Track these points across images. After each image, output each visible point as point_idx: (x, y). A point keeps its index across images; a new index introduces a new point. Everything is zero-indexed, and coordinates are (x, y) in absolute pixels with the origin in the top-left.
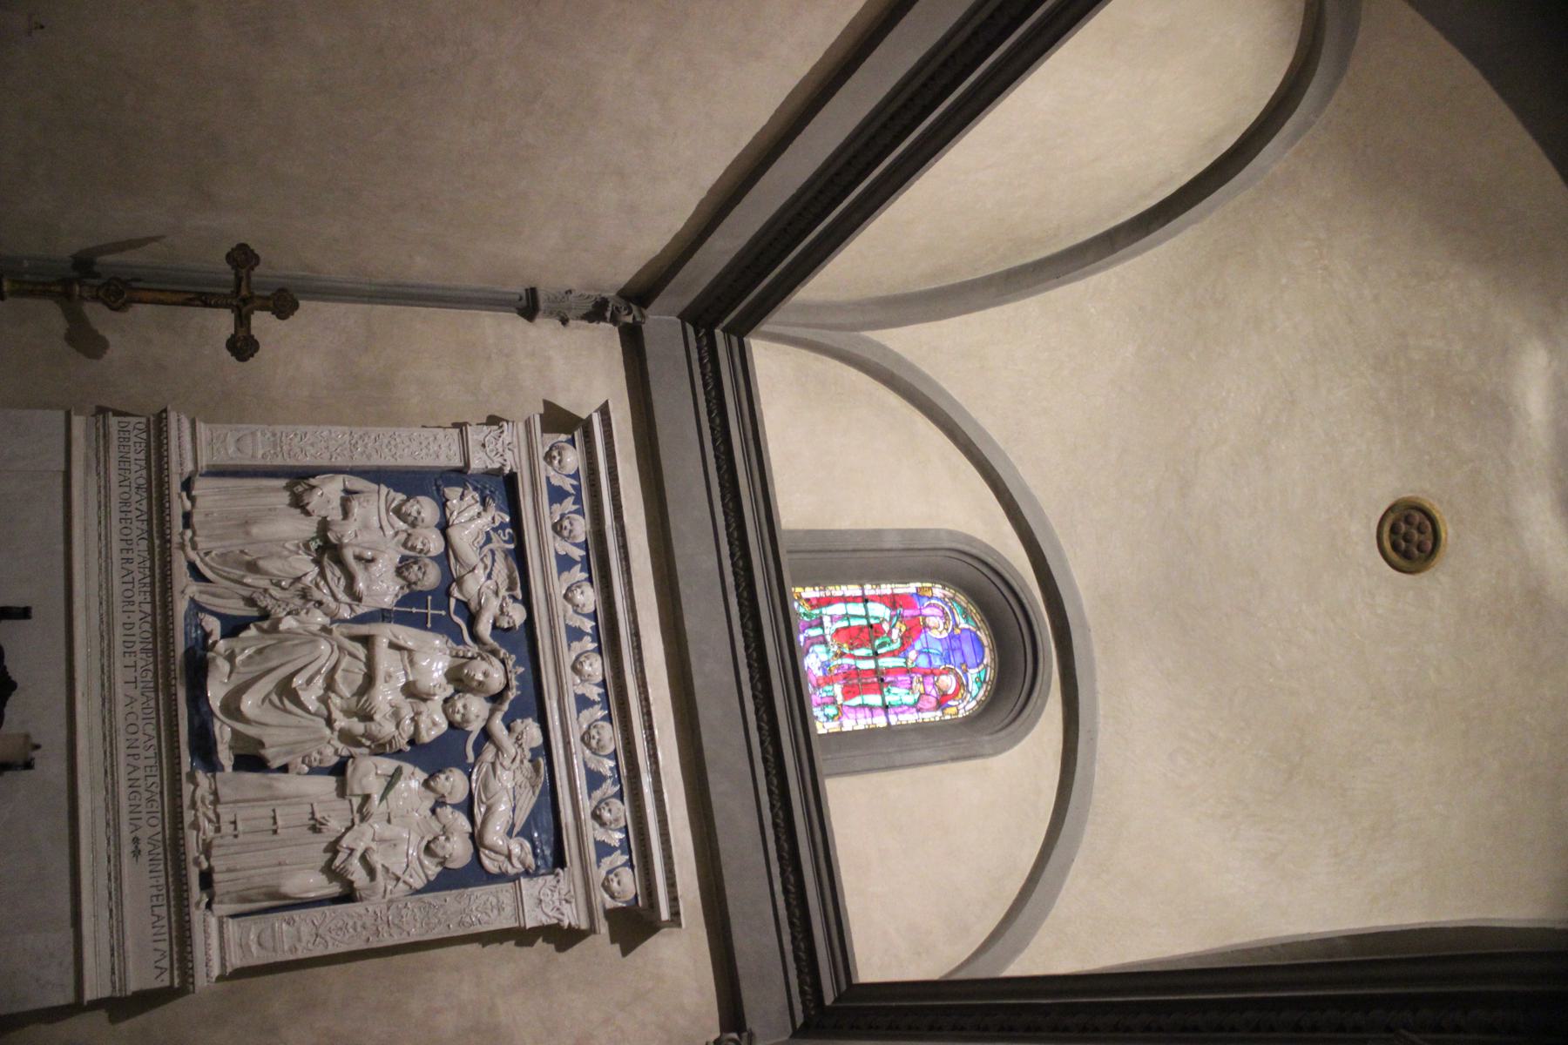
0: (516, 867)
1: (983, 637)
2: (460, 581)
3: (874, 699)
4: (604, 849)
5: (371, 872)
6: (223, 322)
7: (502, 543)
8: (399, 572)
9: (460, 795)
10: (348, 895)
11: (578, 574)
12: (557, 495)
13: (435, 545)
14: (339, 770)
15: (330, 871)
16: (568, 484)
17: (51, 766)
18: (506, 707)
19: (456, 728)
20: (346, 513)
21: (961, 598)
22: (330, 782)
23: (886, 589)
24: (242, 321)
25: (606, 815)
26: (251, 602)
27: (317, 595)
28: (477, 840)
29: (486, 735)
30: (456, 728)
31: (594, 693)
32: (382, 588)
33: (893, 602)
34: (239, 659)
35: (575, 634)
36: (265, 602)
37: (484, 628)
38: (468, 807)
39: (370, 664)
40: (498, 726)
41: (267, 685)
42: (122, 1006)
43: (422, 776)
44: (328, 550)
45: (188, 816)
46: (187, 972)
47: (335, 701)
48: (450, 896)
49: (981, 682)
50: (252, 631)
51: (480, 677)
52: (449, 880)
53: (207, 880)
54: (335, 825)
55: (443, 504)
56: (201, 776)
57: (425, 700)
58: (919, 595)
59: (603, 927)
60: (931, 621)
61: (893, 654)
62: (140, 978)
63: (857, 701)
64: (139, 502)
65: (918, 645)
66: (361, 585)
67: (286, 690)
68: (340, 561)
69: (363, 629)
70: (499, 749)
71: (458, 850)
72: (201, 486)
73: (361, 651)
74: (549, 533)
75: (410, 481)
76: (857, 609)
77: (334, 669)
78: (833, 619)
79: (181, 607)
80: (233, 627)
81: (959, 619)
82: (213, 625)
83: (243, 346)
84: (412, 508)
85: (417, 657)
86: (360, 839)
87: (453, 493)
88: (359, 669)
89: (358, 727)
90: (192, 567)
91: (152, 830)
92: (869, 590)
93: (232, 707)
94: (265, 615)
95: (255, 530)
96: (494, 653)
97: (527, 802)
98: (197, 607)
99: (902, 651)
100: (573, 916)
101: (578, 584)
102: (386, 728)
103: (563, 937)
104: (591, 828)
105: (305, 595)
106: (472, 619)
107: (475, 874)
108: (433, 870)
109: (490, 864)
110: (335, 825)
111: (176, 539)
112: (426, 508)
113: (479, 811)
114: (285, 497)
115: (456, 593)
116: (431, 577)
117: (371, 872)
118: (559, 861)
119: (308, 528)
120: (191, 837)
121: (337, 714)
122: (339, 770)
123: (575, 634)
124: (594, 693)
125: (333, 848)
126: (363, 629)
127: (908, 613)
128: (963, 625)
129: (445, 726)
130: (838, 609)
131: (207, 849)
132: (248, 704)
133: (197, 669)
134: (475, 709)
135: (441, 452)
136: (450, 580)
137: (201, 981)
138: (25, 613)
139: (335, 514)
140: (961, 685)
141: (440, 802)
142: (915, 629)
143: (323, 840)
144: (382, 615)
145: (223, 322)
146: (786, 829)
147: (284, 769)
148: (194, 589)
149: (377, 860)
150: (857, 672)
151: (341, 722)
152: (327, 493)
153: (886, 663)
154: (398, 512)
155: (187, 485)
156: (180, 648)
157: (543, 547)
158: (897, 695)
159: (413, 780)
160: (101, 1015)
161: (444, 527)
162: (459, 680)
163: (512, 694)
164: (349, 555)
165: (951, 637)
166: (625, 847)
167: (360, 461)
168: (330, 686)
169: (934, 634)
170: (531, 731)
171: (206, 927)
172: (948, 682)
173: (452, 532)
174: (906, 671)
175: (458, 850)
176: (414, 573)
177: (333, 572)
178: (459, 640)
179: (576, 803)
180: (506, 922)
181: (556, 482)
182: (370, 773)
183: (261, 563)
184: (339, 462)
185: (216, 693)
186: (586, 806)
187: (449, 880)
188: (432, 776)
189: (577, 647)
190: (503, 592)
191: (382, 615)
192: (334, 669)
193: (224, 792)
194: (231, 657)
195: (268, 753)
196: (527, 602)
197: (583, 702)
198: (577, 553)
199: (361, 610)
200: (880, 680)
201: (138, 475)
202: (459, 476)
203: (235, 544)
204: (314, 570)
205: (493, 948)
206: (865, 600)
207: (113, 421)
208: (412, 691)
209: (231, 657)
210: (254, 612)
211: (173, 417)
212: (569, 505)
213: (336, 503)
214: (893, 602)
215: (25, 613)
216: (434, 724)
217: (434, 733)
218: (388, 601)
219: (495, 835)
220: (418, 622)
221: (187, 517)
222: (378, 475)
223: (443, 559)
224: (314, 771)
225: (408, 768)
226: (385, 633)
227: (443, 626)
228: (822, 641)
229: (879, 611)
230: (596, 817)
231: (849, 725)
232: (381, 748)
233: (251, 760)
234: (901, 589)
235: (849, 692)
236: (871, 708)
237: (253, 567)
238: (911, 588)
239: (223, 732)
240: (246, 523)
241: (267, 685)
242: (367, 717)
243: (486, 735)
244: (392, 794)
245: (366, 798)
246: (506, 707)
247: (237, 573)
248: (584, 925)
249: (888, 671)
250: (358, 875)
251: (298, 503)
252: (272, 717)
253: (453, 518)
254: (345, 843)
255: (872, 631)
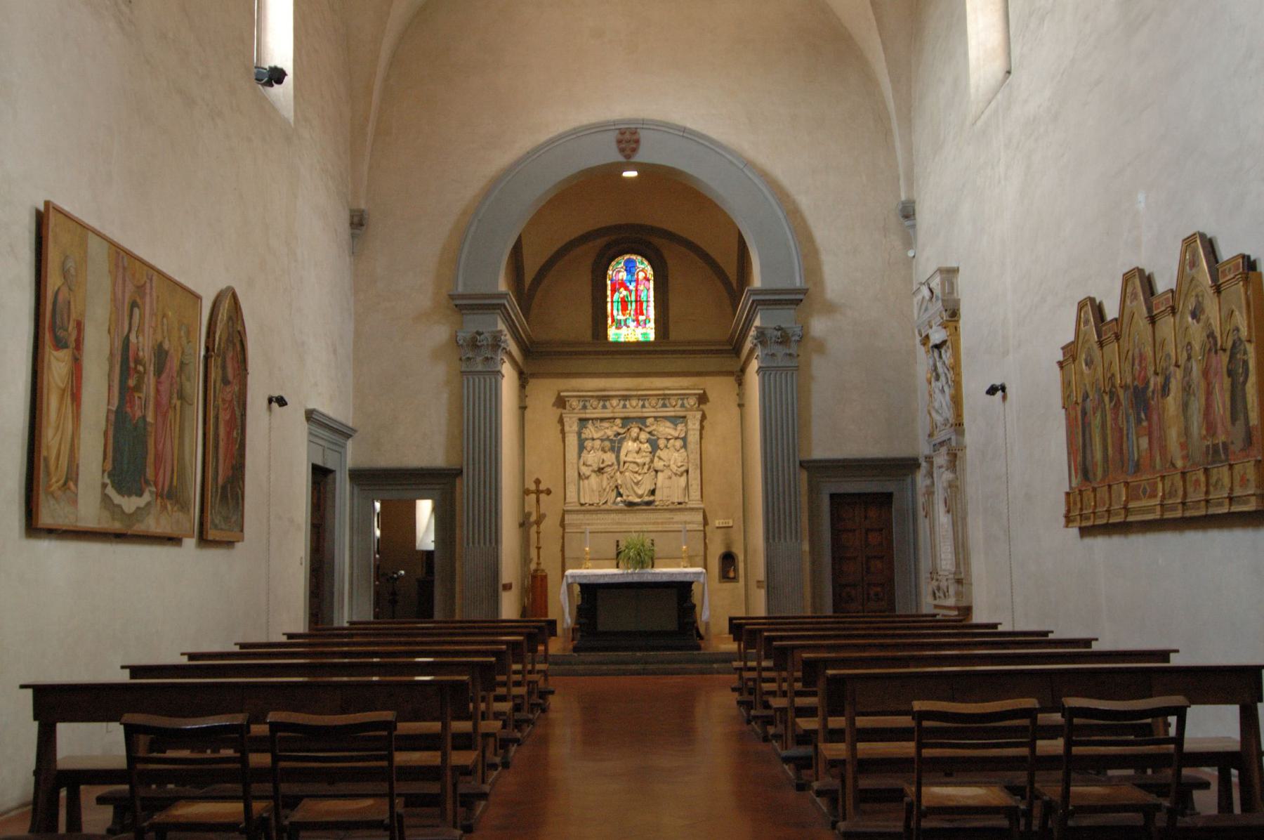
0: (684, 428)
1: (627, 257)
2: (608, 437)
3: (645, 305)
4: (683, 405)
5: (682, 466)
6: (543, 497)
7: (598, 424)
8: (605, 452)
9: (665, 441)
10: (687, 471)
11: (607, 404)
12: (585, 407)
13: (598, 443)
14: (657, 471)
15: (681, 475)
16: (581, 404)
17: (652, 536)
18: (643, 427)
19: (648, 441)
20: (590, 466)
21: (613, 263)
22: (659, 474)
23: (609, 293)
24: (542, 492)
25: (674, 403)
26: (613, 490)
27: (612, 474)
28: (677, 438)
29: (650, 433)
30: (648, 441)
31: (641, 403)
32: (610, 457)
33: (613, 291)
34: (628, 493)
35: (624, 406)
36: (613, 487)
37: (622, 431)
38: (668, 440)
39: (631, 462)
40: (648, 430)
41: (636, 488)
42: (706, 523)
43: (659, 451)
44: (600, 471)
45: (665, 507)
46: (700, 509)
47: (640, 471)
48: (688, 445)
49: (642, 263)
50: (621, 491)
51: (636, 435)
52: (685, 446)
53: (680, 503)
54: (670, 473)
55: (587, 439)
56: (657, 503)
57: (640, 449)
58: (611, 280)
59: (701, 406)
60: (620, 278)
61: (630, 295)
62: (700, 518)
63: (645, 311)
64: (588, 516)
65: (628, 284)
66: (610, 463)
67: (637, 483)
68: (603, 469)
69: (622, 464)
70: (654, 430)
71: (679, 443)
72: (582, 501)
73: (627, 465)
74: (596, 411)
75: (581, 447)
76: (615, 304)
77: (633, 472)
78: (618, 315)
79: (614, 507)
80: (620, 495)
81: (620, 266)
82: (619, 499)
83: (548, 492)
84: (589, 449)
85: (630, 449)
86: (674, 467)
87: (583, 436)
88: (632, 465)
89: (647, 466)
90: (604, 504)
91: (667, 515)
92: (609, 299)
93: (641, 496)
94: (617, 487)
95: (595, 487)
96: (628, 430)
97: (668, 424)
98: (614, 502)
99: (630, 292)
100: (699, 415)
101: (611, 404)
102: (648, 460)
103: (704, 417)
104: (677, 408)
105: (612, 477)
106: (619, 434)
107: (684, 439)
108: (683, 450)
109: (682, 435)
110: (670, 473)
111: (598, 508)
112: (588, 444)
113: (670, 437)
114: (586, 481)
115: (610, 438)
116: (607, 444)
117: (682, 466)
118: (684, 417)
119: (593, 475)
120: (670, 507)
121: (643, 472)
122: (657, 471)
123: (624, 406)
124: (641, 403)
125: (676, 474)
126: (622, 464)
127: (617, 286)
128: (622, 265)
129: (647, 445)
130: (615, 312)
131: (673, 503)
132: (640, 492)
133: (631, 504)
134: (643, 436)
135: (572, 440)
136: (608, 439)
137: (702, 506)
138: (618, 541)
139: (591, 468)
140: (642, 271)
141: (666, 447)
142: (623, 284)
143: (674, 477)
144: (618, 457)
145: (543, 497)
146: (684, 352)
147: (655, 484)
148: (609, 504)
149: (679, 464)
150: (636, 309)
151: (645, 470)
152: (584, 470)
153: (633, 298)
154: (589, 452)
155: (582, 505)
156: (626, 508)
157: (599, 413)
158: (643, 297)
159: (659, 453)
160: (707, 528)
161: (593, 439)
162: (636, 439)
163: (640, 426)
164: (602, 466)
165: (626, 270)
166: (682, 399)
167: (575, 461)
168: (636, 472)
169: (625, 278)
170: (649, 421)
171: (690, 505)
172: (641, 275)
173: (596, 436)
174: (637, 290)
175: (679, 443)
176: (607, 449)
177: (606, 470)
178: (625, 438)
179: (670, 412)
180: (698, 433)
181: (580, 407)
182: (658, 464)
183: (604, 487)
184: (576, 466)
185: (638, 500)
186: (672, 409)
187: (685, 446)
188: (659, 448)
189: (628, 406)
190: (612, 425)
191: (618, 457)
192: (633, 472)
193: (660, 498)
194: (628, 496)
195: (652, 488)
196: (615, 418)
197: (643, 406)
198: (601, 403)
199: (616, 463)
200: (639, 302)
201: (581, 516)
202: (579, 434)
203: (597, 493)
204: (605, 475)
205: (703, 436)
206: (612, 302)
207: (566, 522)
208: (638, 452)
209: (628, 496)
210: (615, 491)
211: (565, 508)
212: (587, 404)
213: (587, 468)
214: (613, 291)
215: (618, 541)
216: (646, 447)
217: (649, 447)
218: (613, 456)
219: (676, 435)
220: (619, 449)
221: (590, 505)
222: (580, 457)
223: (602, 440)
224: (656, 477)
225: (657, 454)
226: (623, 458)
227: (621, 441)
228: (625, 321)
229: (616, 296)
230: (674, 407)
231: (652, 316)
232: (652, 461)
233: (653, 492)
234: (609, 287)
235: (642, 314)
236: (648, 306)
237: (605, 490)
238: (609, 282)
239: (647, 499)
240: (593, 491)
241: (636, 488)
242: (645, 464)
243: (650, 433)
244: (665, 459)
245: (664, 465)
246: (643, 427)
247: (605, 493)
248: (701, 413)
249: (636, 298)
250: (683, 469)
251: (587, 478)
252: (643, 486)
253: (590, 436)
254: (675, 471)
255: (624, 303)
